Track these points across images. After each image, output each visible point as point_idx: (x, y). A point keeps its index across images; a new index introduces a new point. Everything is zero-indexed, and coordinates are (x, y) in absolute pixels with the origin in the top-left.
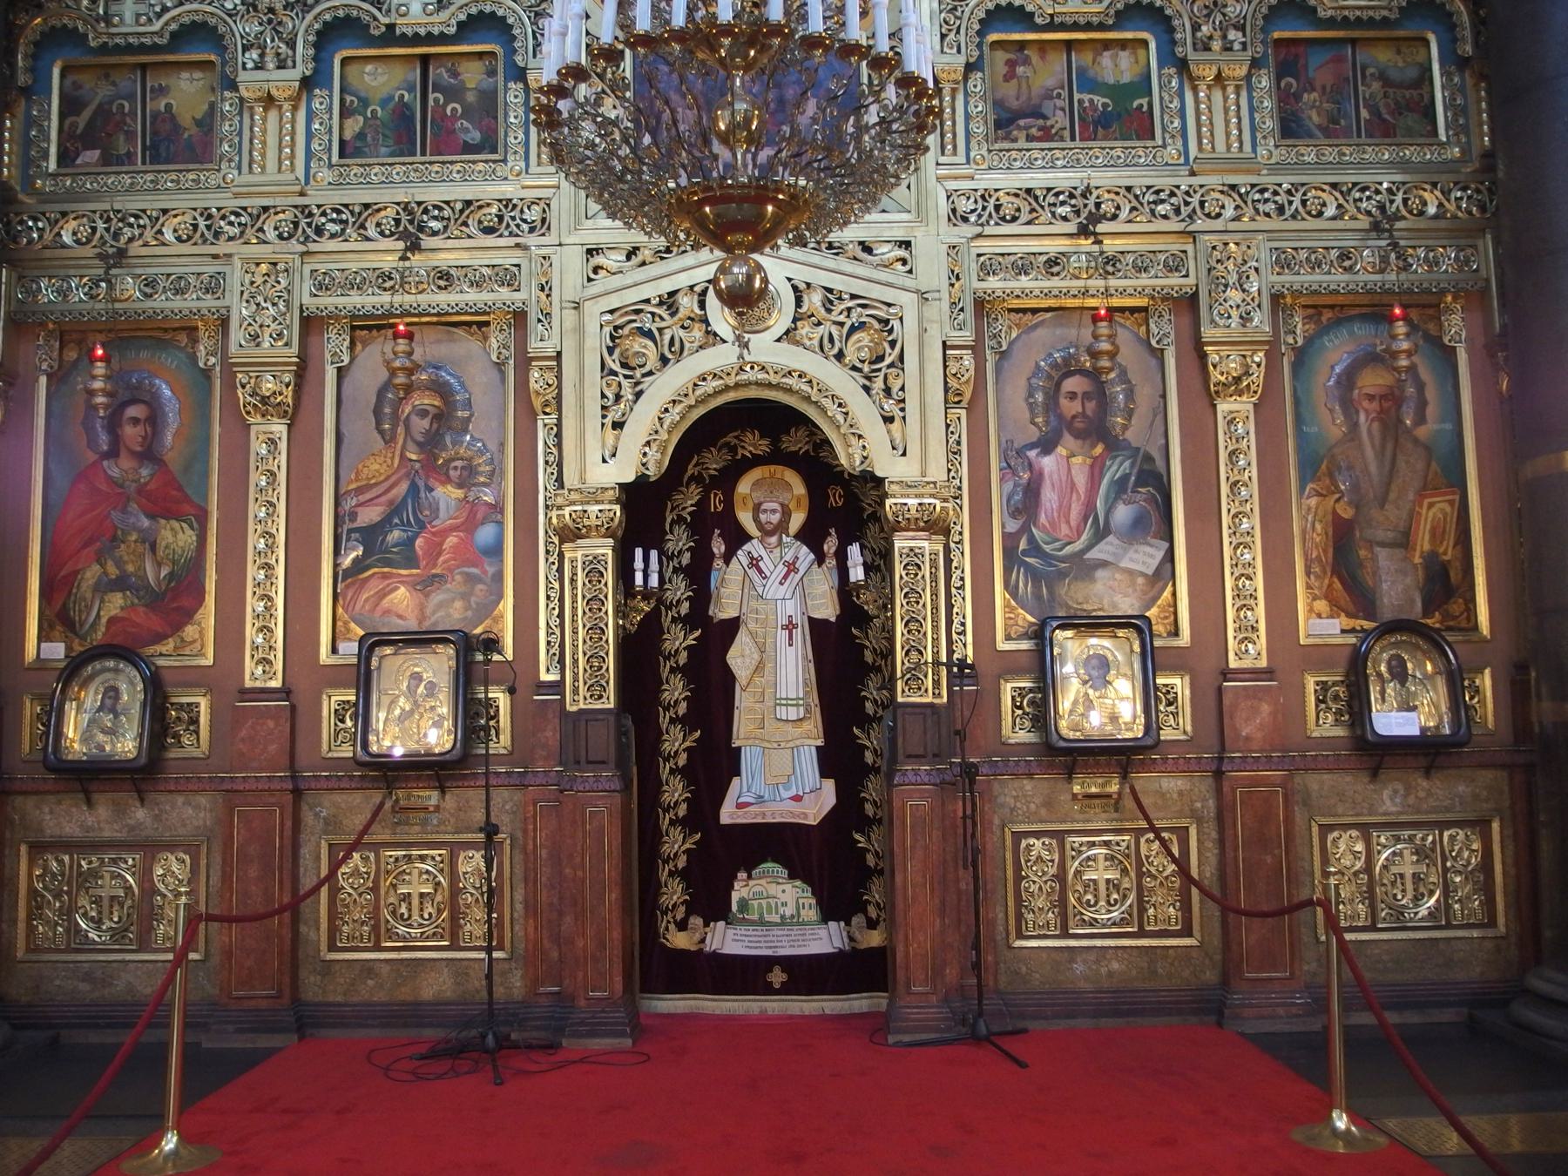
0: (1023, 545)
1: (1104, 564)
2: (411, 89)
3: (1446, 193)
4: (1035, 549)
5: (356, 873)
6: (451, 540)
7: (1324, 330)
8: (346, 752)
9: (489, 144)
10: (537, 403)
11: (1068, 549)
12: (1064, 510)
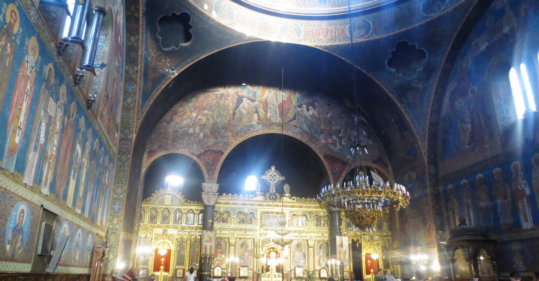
9: (251, 223)
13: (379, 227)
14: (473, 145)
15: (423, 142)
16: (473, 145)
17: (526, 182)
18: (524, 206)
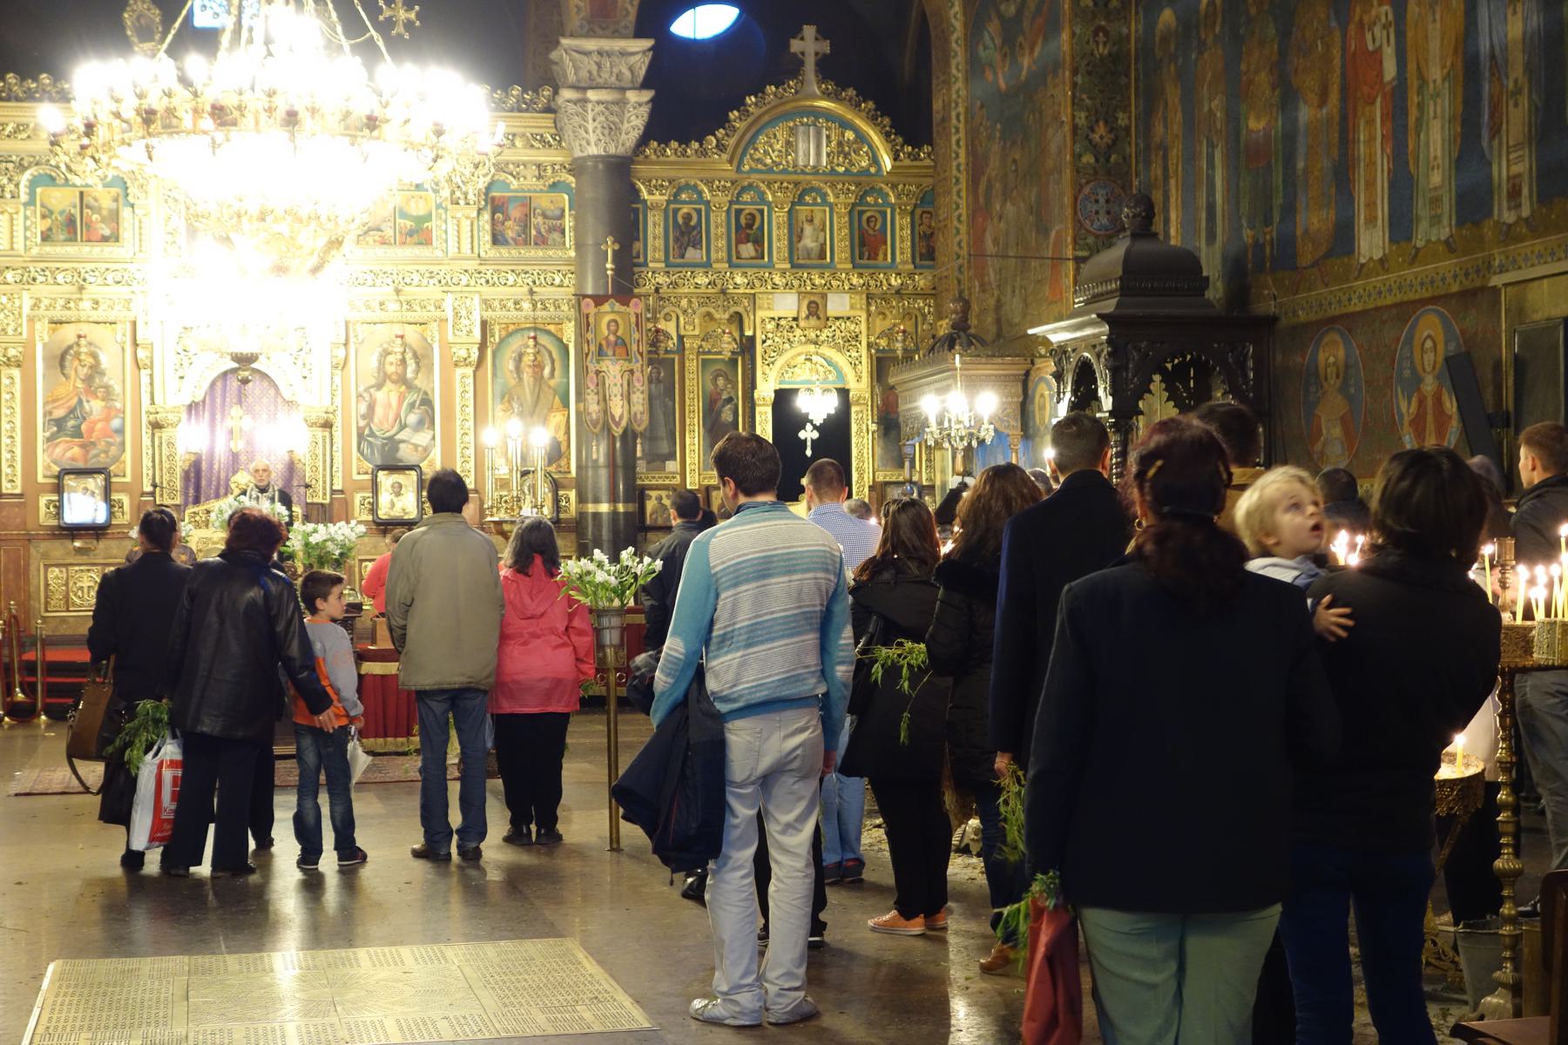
0: (367, 432)
1: (403, 441)
2: (75, 207)
3: (564, 276)
4: (372, 434)
5: (57, 578)
6: (99, 426)
7: (510, 335)
8: (54, 522)
9: (115, 238)
10: (141, 364)
11: (388, 434)
12: (386, 417)
13: (862, 243)
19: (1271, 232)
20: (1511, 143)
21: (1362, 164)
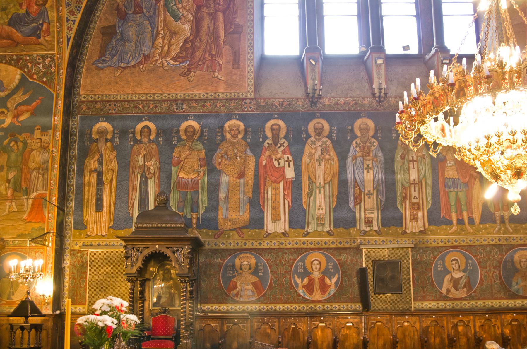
14: (186, 64)
15: (72, 13)
16: (186, 64)
17: (291, 158)
18: (276, 195)
19: (197, 215)
20: (366, 208)
21: (270, 202)
